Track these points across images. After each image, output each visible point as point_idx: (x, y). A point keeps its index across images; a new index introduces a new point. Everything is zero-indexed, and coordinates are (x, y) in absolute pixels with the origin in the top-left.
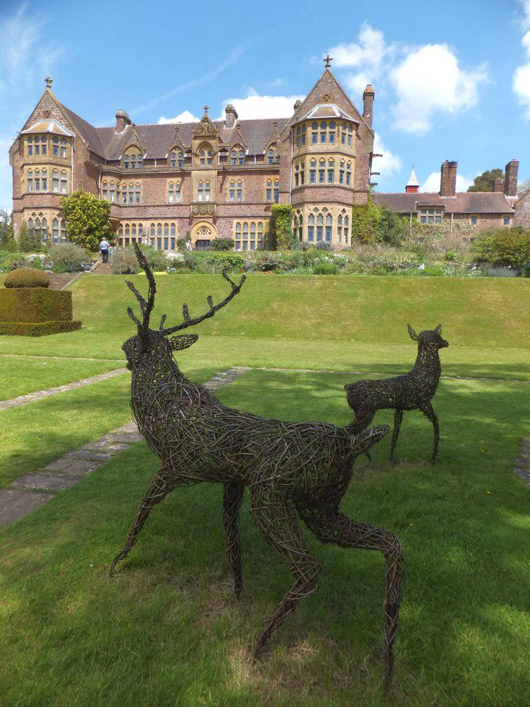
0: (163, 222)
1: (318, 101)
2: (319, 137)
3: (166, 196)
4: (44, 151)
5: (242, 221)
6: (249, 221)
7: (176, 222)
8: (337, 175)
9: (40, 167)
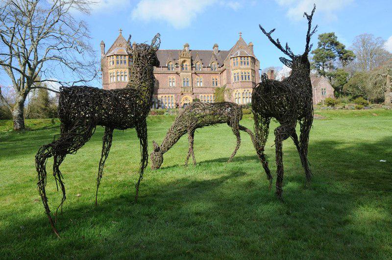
0: (167, 96)
1: (238, 49)
2: (243, 63)
3: (168, 83)
4: (125, 62)
5: (203, 95)
6: (206, 95)
7: (174, 96)
8: (251, 77)
9: (123, 70)
